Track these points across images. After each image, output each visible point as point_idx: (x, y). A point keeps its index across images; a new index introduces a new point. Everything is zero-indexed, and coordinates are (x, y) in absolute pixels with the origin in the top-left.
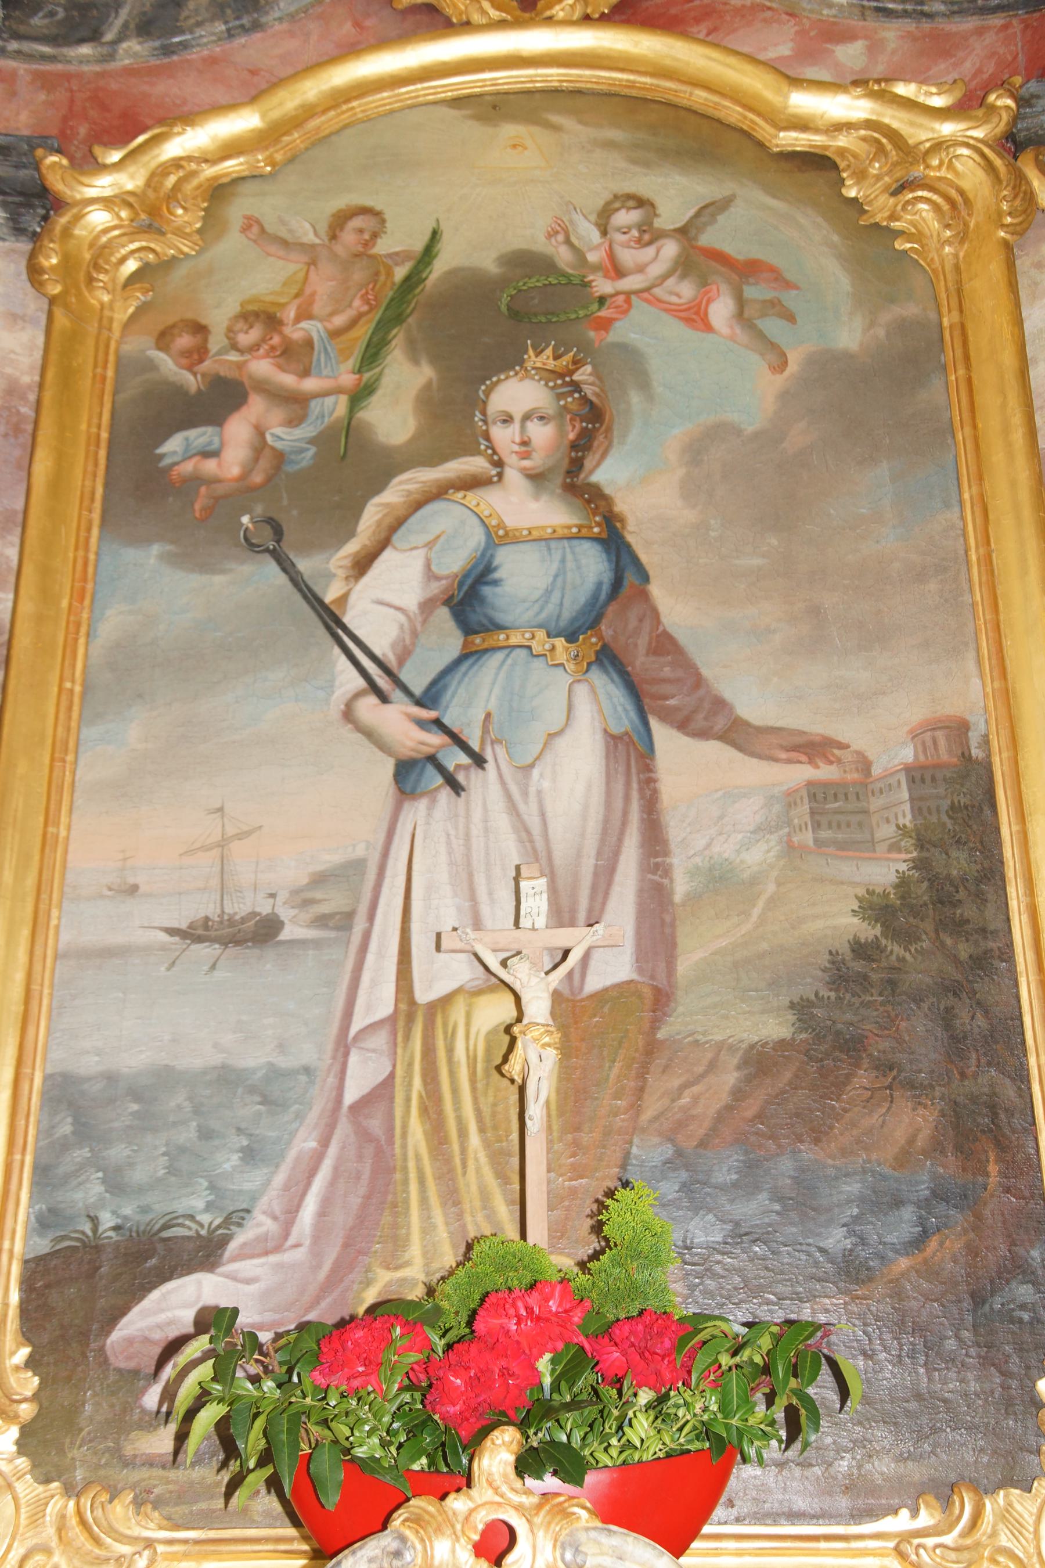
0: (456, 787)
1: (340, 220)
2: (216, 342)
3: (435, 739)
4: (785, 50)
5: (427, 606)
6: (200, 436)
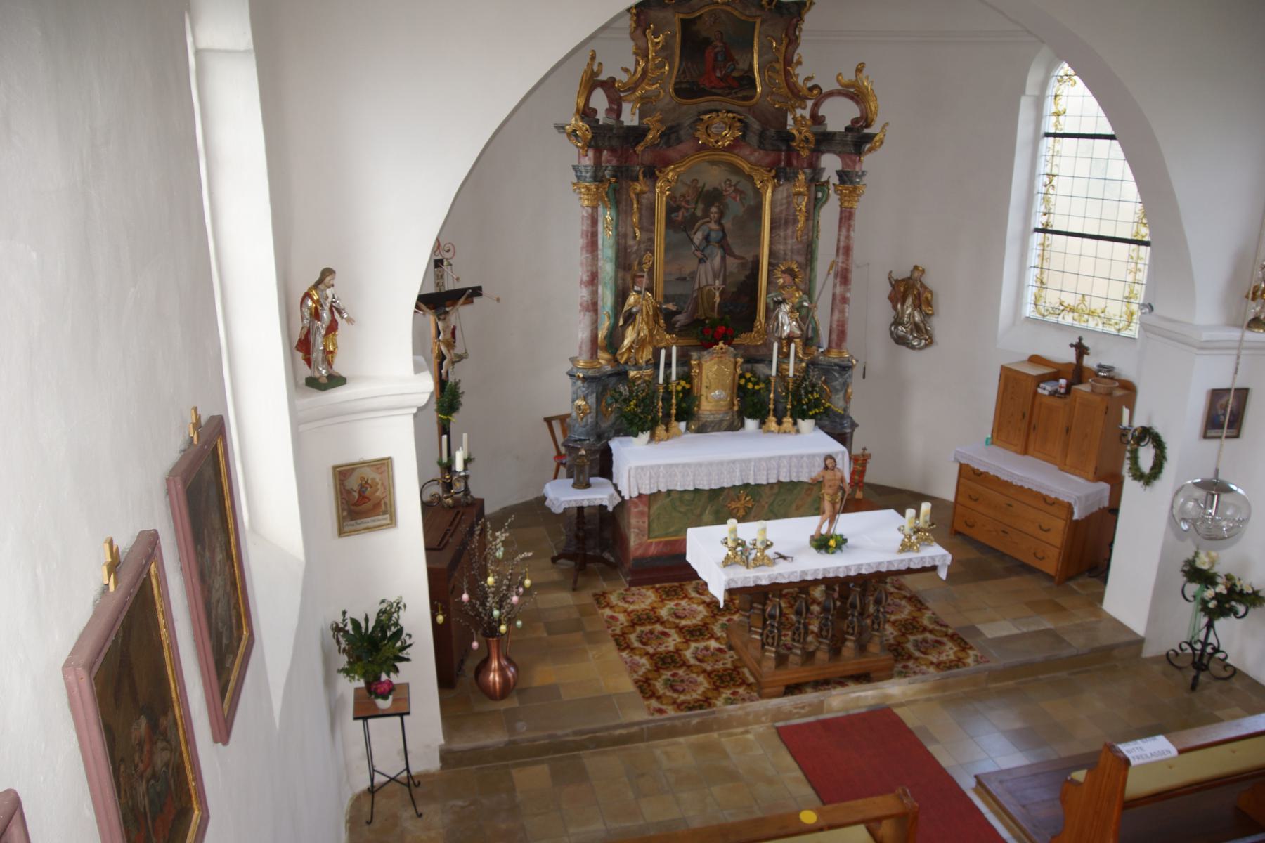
0: (705, 262)
1: (694, 180)
2: (678, 199)
3: (703, 256)
4: (748, 153)
5: (703, 239)
6: (676, 214)
